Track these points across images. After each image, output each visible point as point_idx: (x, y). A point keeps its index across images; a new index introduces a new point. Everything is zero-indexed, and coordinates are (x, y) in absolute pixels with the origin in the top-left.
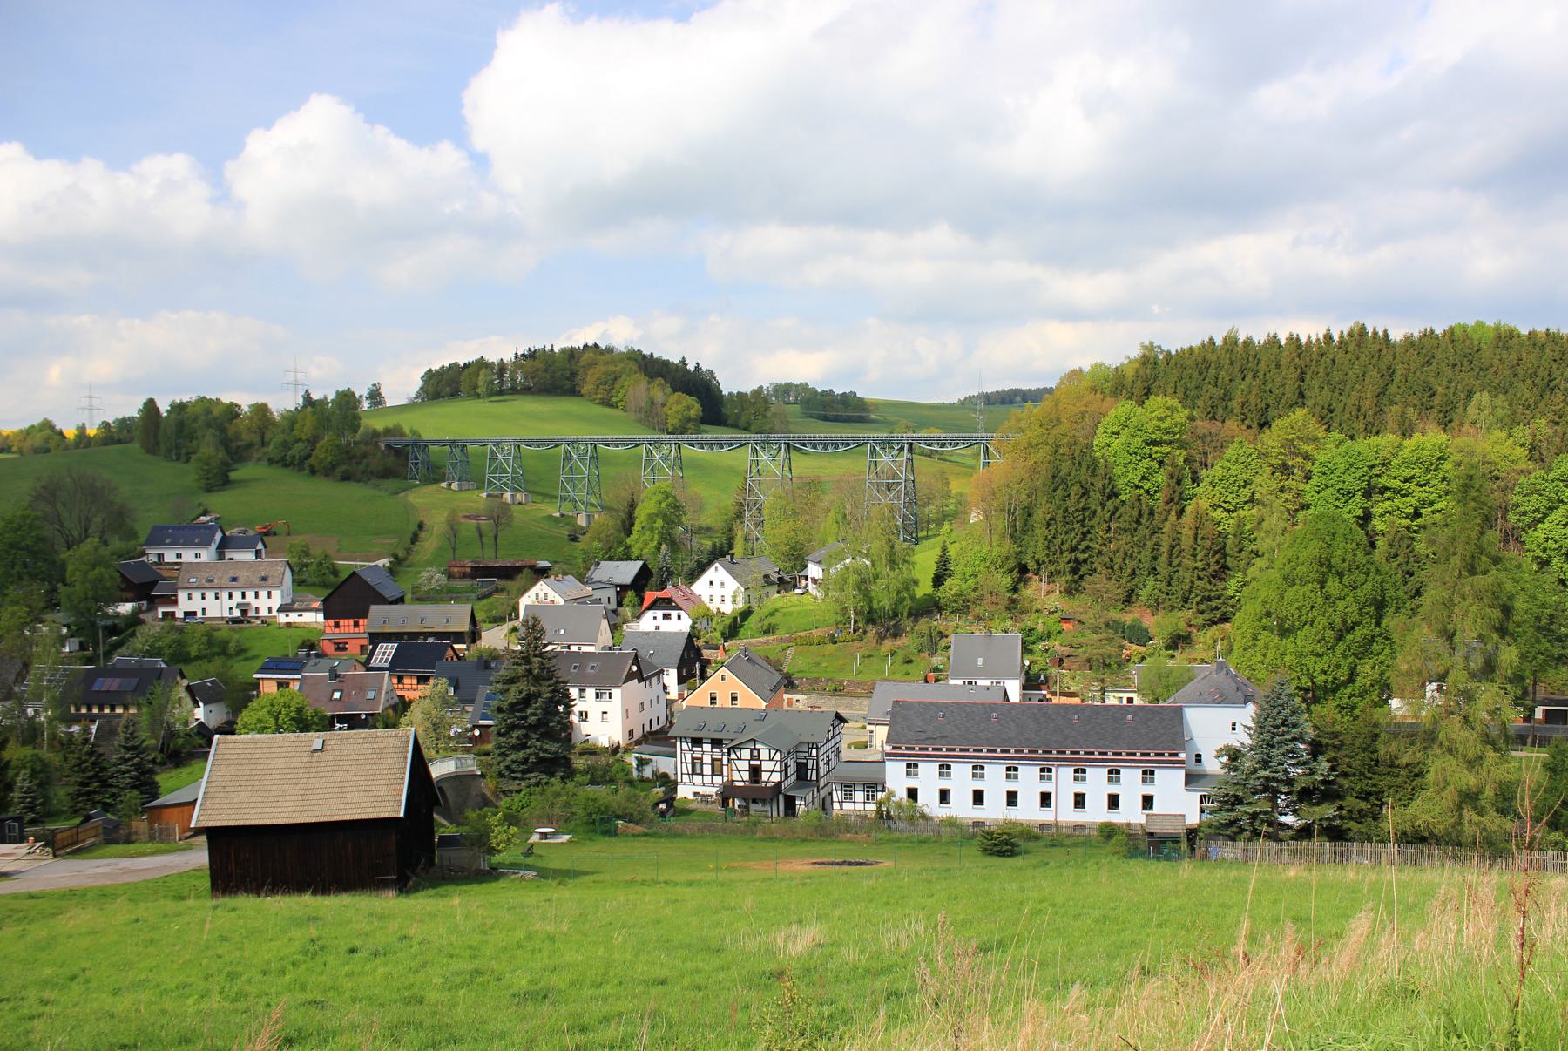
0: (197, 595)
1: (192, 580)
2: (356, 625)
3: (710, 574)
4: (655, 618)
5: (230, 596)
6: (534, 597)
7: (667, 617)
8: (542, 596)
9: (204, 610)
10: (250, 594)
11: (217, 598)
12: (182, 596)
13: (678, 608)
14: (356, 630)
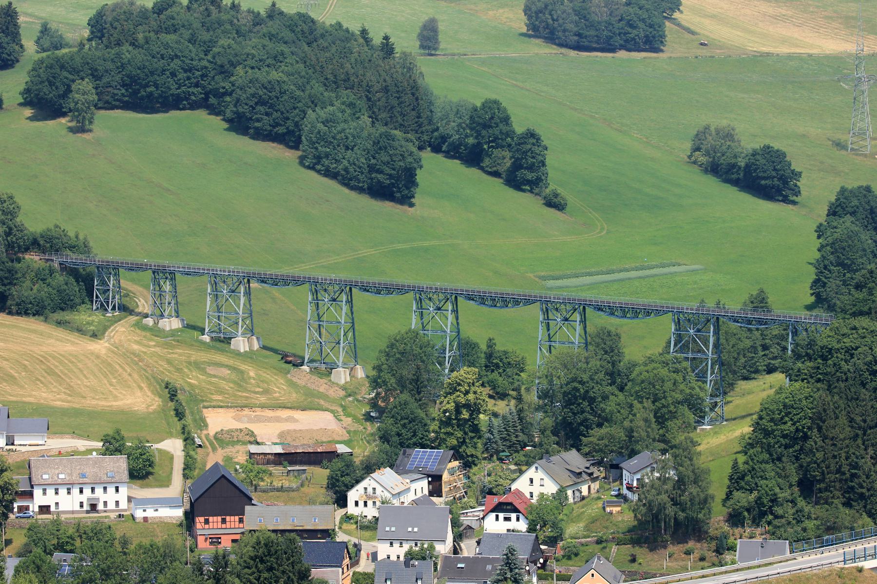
0: (51, 491)
1: (45, 477)
2: (224, 521)
3: (531, 472)
4: (497, 518)
5: (81, 491)
6: (363, 491)
7: (507, 519)
8: (370, 491)
9: (57, 504)
10: (99, 491)
11: (69, 493)
12: (37, 492)
13: (516, 510)
14: (224, 526)
